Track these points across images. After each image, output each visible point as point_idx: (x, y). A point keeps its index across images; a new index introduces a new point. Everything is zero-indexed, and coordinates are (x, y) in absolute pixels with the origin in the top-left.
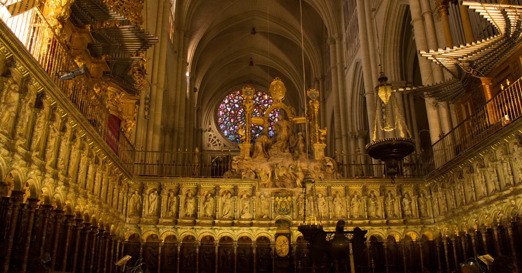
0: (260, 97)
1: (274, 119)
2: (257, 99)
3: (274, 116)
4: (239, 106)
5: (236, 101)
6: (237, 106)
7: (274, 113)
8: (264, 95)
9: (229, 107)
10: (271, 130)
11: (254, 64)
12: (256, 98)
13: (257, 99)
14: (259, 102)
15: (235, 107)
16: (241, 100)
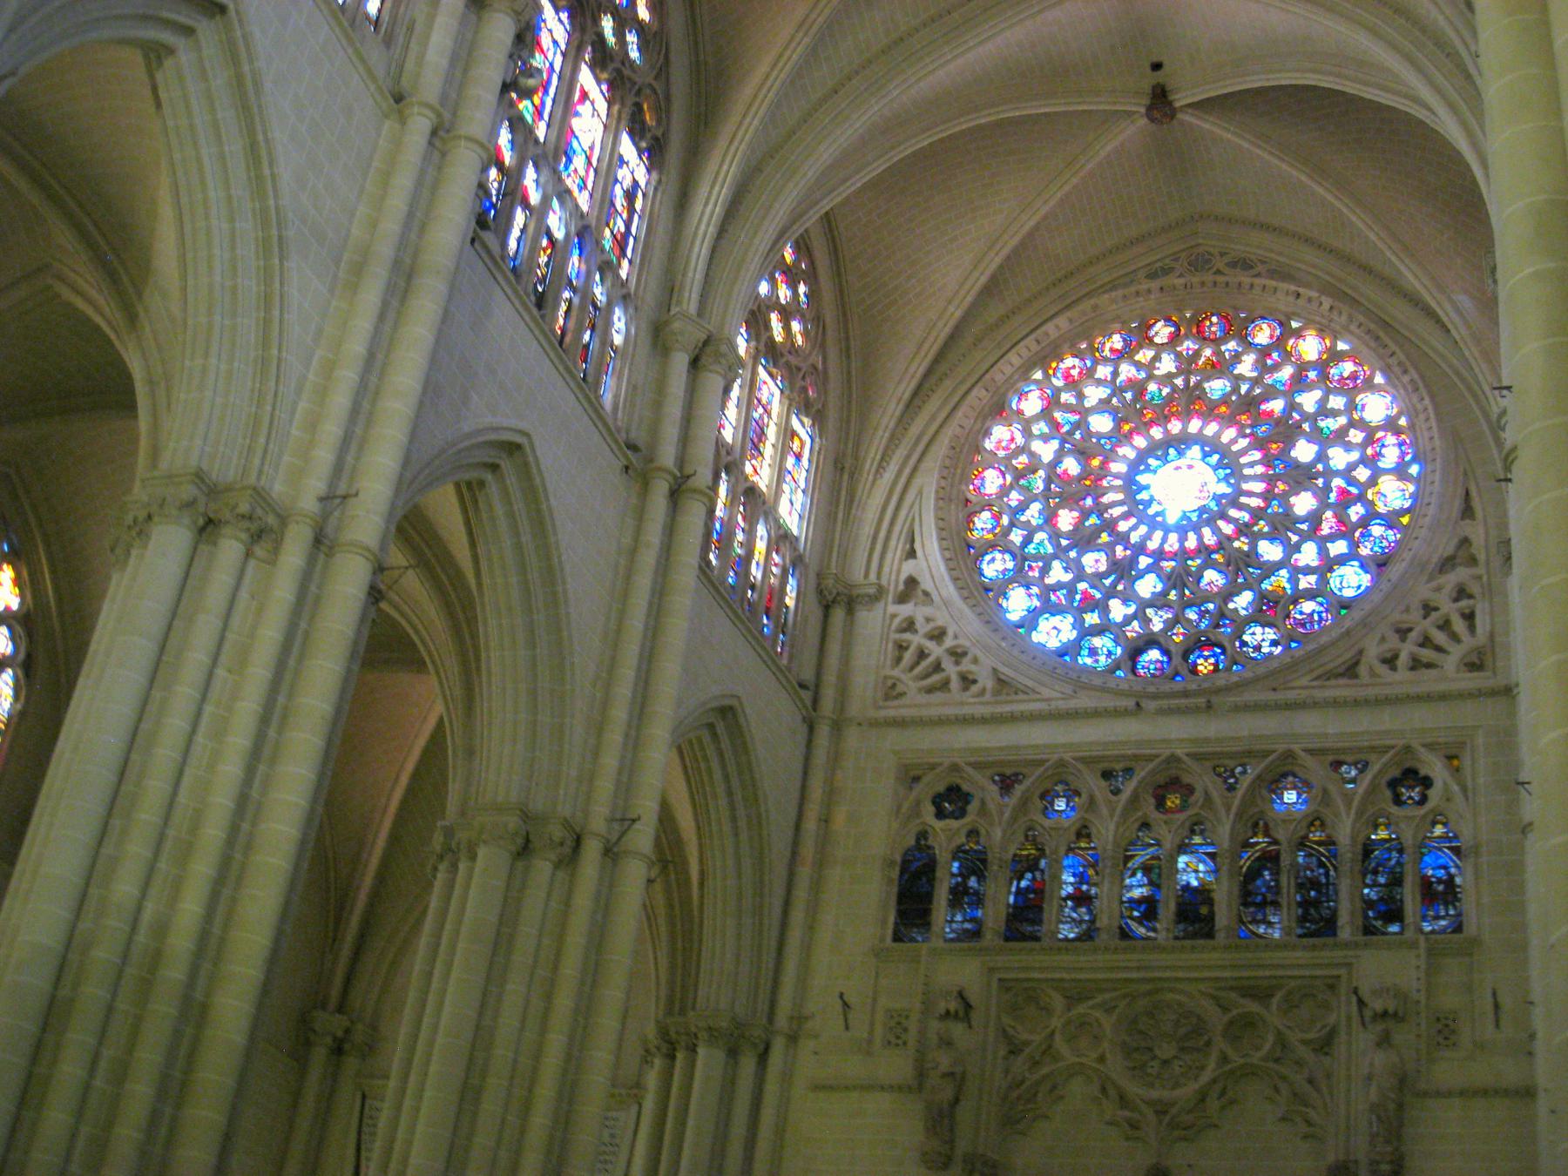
0: (1264, 352)
1: (1373, 481)
2: (1246, 367)
3: (1371, 461)
4: (1118, 422)
5: (1094, 394)
6: (1101, 423)
7: (1370, 440)
8: (1298, 334)
9: (1045, 439)
10: (1342, 560)
11: (1180, 99)
12: (1237, 358)
13: (1246, 367)
14: (1255, 382)
15: (1088, 434)
16: (1131, 383)
